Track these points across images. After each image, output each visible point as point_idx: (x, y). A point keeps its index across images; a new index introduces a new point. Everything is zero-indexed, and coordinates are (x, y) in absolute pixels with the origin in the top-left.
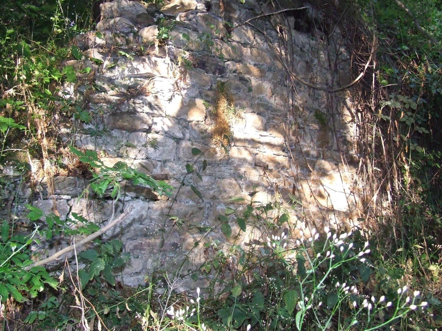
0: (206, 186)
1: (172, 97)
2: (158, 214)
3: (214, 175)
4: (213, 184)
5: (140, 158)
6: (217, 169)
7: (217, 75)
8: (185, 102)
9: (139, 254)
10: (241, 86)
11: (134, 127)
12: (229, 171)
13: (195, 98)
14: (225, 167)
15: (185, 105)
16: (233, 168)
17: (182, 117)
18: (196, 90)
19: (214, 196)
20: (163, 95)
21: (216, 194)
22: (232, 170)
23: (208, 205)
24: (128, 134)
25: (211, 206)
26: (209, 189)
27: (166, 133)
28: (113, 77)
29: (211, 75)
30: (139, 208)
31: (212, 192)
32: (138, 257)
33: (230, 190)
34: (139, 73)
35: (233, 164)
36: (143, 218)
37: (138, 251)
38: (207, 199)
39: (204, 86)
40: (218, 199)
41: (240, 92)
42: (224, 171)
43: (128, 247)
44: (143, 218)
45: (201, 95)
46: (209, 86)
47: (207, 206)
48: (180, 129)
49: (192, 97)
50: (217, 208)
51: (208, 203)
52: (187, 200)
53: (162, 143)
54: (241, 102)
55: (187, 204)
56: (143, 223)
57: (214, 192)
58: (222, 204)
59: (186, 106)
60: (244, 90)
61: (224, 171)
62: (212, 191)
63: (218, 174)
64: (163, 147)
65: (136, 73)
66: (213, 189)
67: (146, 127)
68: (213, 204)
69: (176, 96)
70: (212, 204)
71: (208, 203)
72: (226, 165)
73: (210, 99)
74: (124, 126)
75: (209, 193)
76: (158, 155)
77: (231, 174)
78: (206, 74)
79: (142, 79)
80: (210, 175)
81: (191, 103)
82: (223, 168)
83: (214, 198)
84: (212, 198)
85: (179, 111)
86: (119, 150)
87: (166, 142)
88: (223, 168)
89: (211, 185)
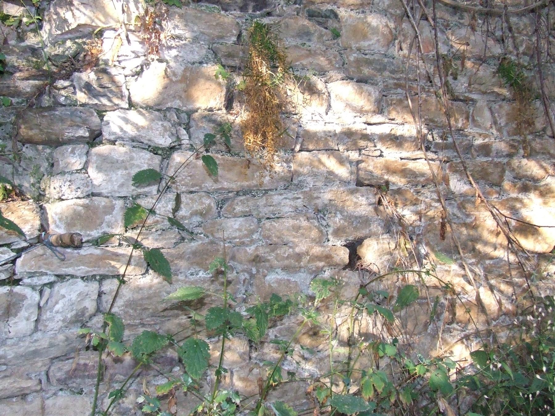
0: (235, 238)
1: (142, 66)
2: (122, 303)
3: (255, 213)
4: (252, 232)
5: (70, 197)
6: (262, 202)
7: (250, 11)
8: (175, 74)
9: (82, 386)
10: (312, 29)
11: (53, 137)
12: (292, 203)
13: (201, 63)
14: (281, 194)
15: (174, 79)
16: (300, 196)
17: (169, 105)
18: (201, 47)
19: (257, 256)
20: (123, 64)
21: (261, 252)
22: (299, 200)
23: (244, 276)
24: (48, 151)
25: (252, 276)
26: (243, 243)
27: (133, 140)
28: (38, 44)
29: (238, 13)
30: (74, 296)
31: (250, 250)
32: (81, 392)
33: (296, 240)
34: (70, 28)
35: (302, 187)
36: (87, 314)
37: (79, 380)
38: (241, 263)
39: (222, 37)
40: (268, 261)
41: (309, 40)
42: (280, 203)
43: (54, 375)
44: (87, 314)
45: (215, 55)
46: (233, 35)
47: (243, 277)
48: (165, 130)
49: (194, 63)
50: (268, 278)
51: (243, 271)
52: (192, 270)
53: (123, 161)
54: (315, 62)
55: (192, 278)
56: (89, 324)
57: (257, 249)
58: (279, 270)
59: (177, 82)
60: (321, 36)
61: (280, 203)
62: (253, 248)
63: (265, 211)
64: (126, 169)
65: (67, 29)
66: (252, 242)
67: (83, 132)
68: (258, 271)
69: (155, 64)
70: (254, 271)
71: (243, 271)
72: (283, 192)
73: (236, 62)
74: (31, 136)
75: (246, 251)
76: (116, 188)
77: (297, 208)
78: (223, 12)
79: (84, 40)
80: (246, 215)
81: (188, 74)
82: (276, 198)
83: (257, 260)
84: (254, 260)
85: (161, 93)
86: (39, 182)
87: (132, 158)
88: (276, 197)
89: (246, 236)
